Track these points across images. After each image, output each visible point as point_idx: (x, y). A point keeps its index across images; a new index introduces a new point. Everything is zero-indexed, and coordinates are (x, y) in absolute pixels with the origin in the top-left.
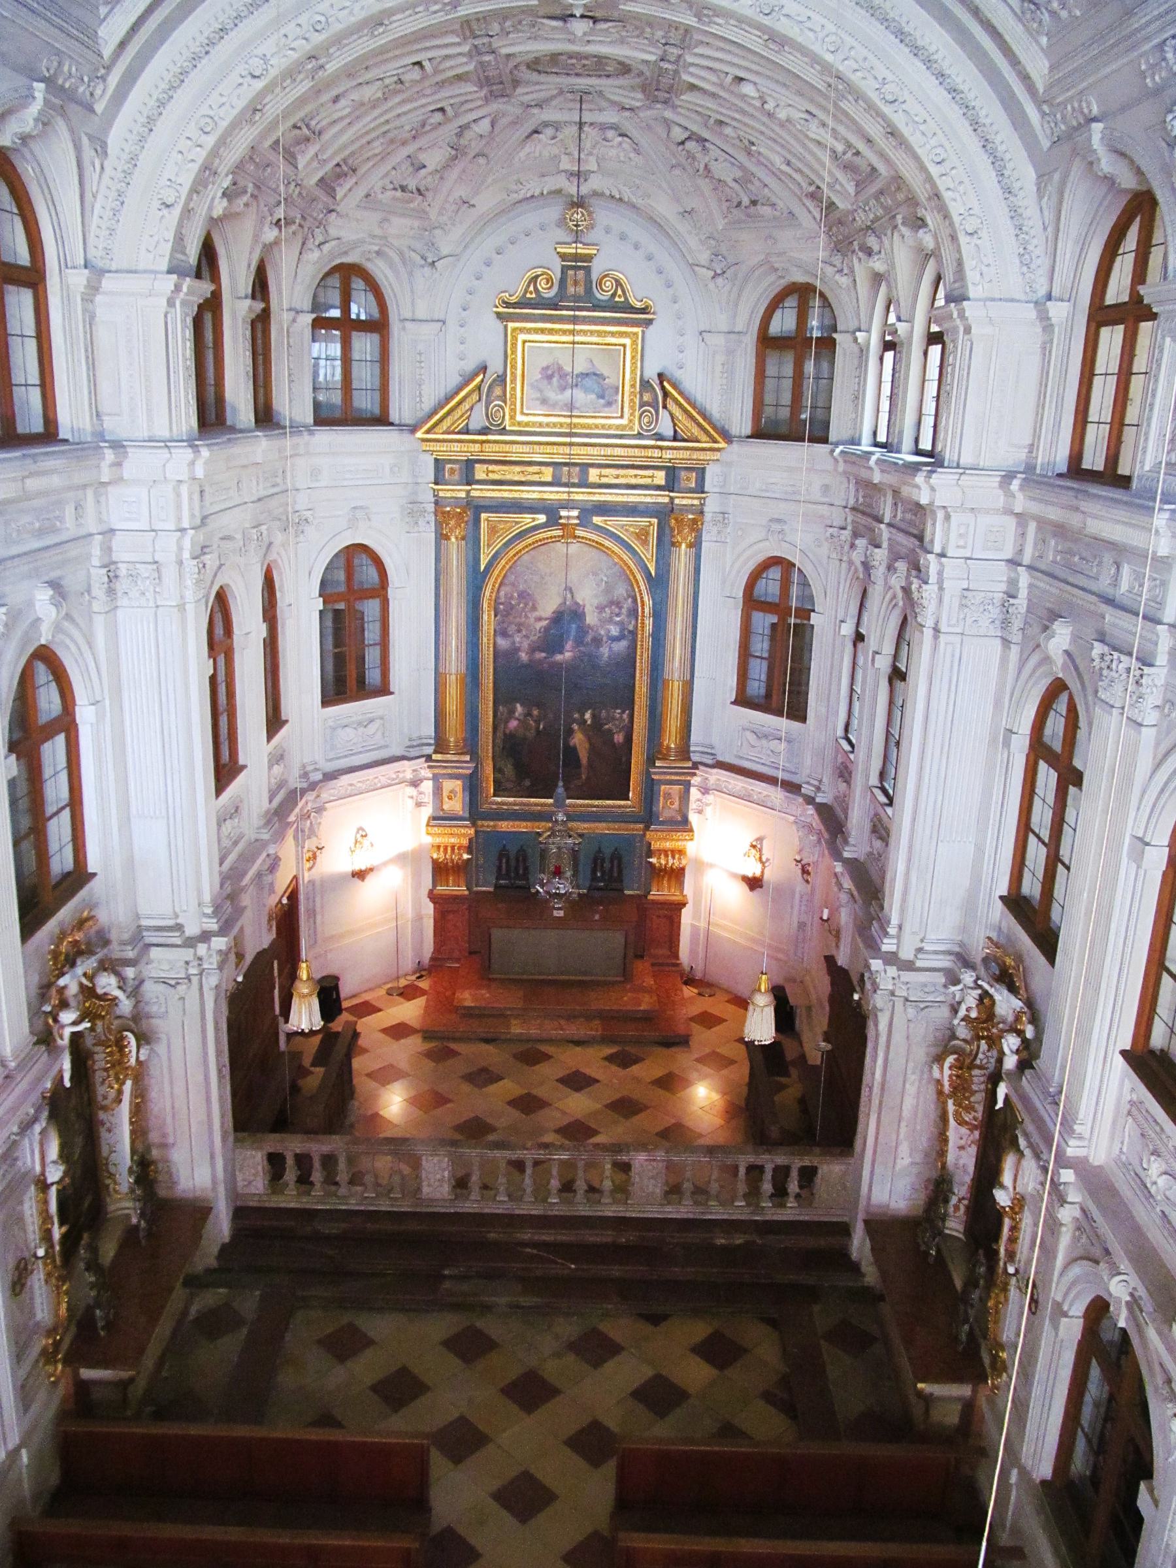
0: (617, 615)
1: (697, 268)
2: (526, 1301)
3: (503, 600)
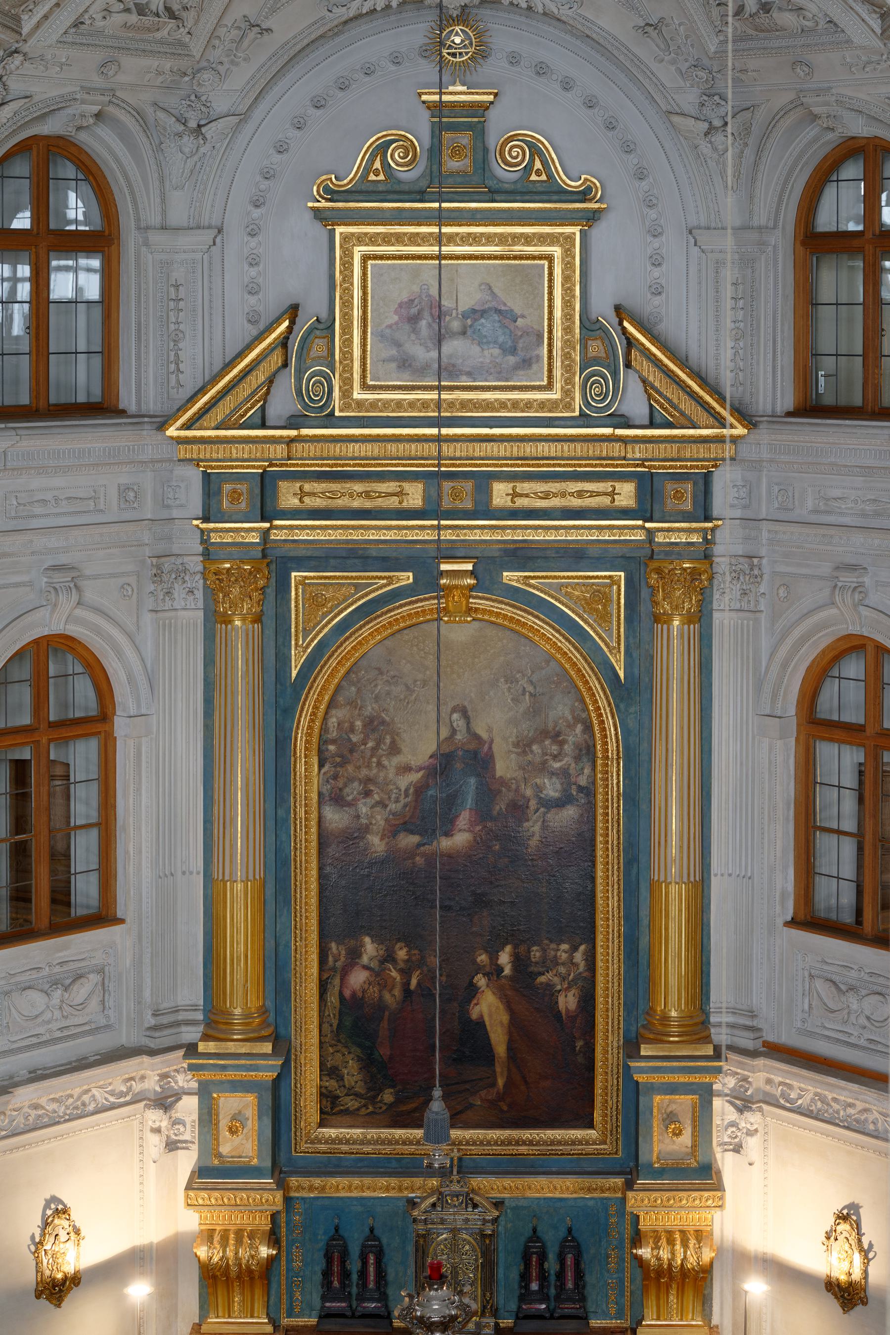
0: (555, 757)
3: (333, 734)
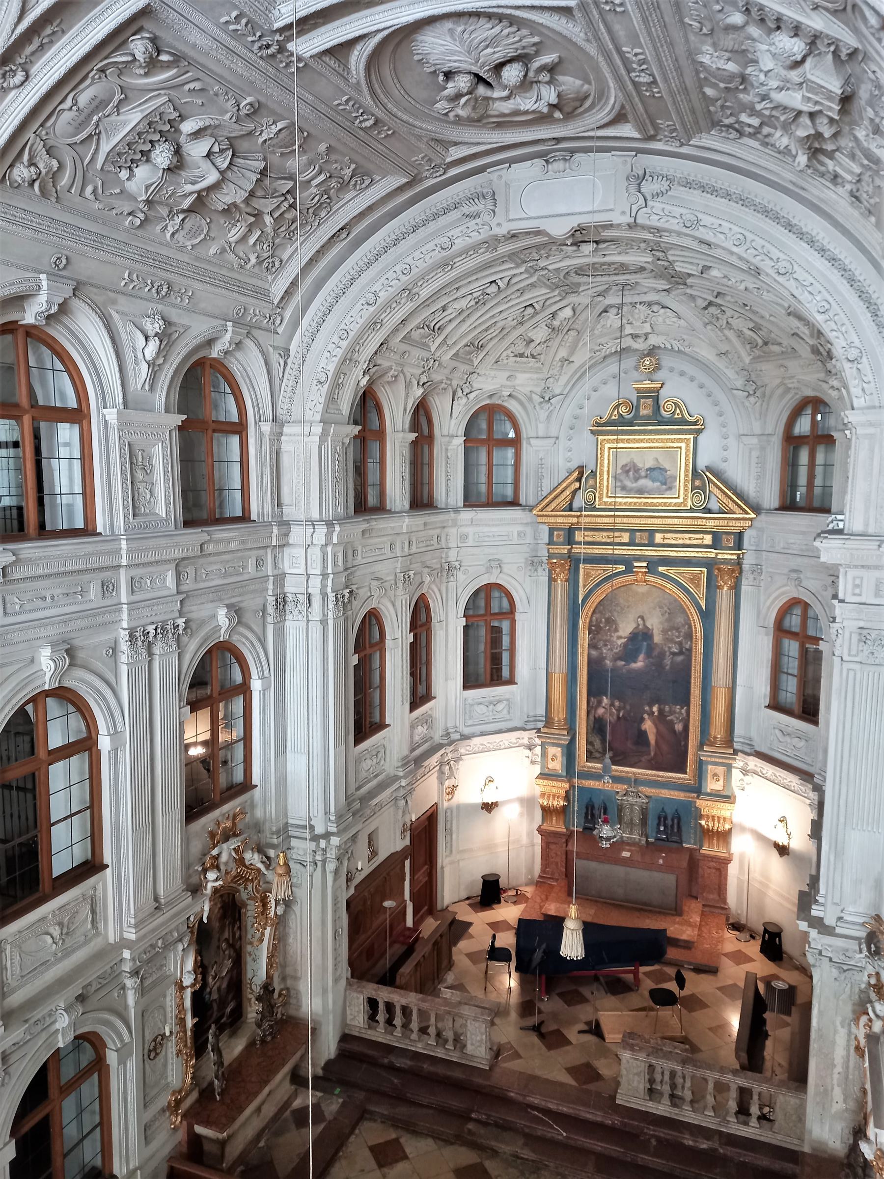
0: (678, 637)
1: (735, 392)
2: (526, 1154)
